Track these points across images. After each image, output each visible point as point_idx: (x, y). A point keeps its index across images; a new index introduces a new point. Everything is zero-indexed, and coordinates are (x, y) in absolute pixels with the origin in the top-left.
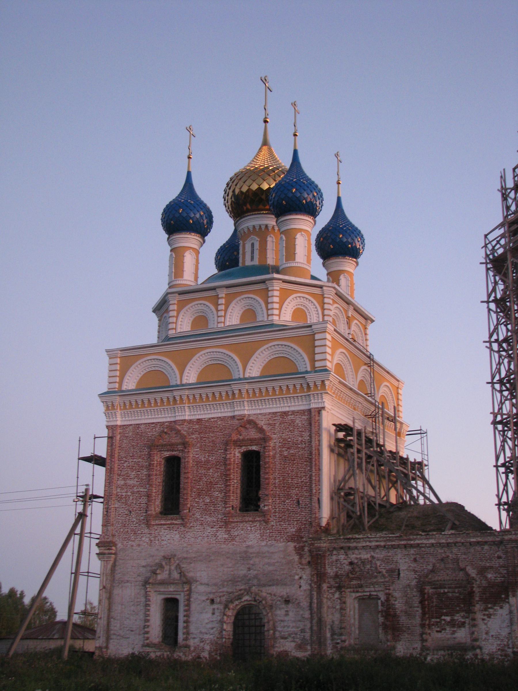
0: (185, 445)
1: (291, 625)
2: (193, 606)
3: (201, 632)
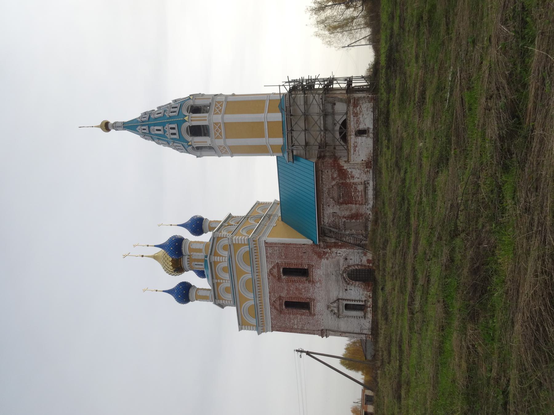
0: (280, 298)
1: (356, 257)
2: (348, 298)
3: (359, 295)
